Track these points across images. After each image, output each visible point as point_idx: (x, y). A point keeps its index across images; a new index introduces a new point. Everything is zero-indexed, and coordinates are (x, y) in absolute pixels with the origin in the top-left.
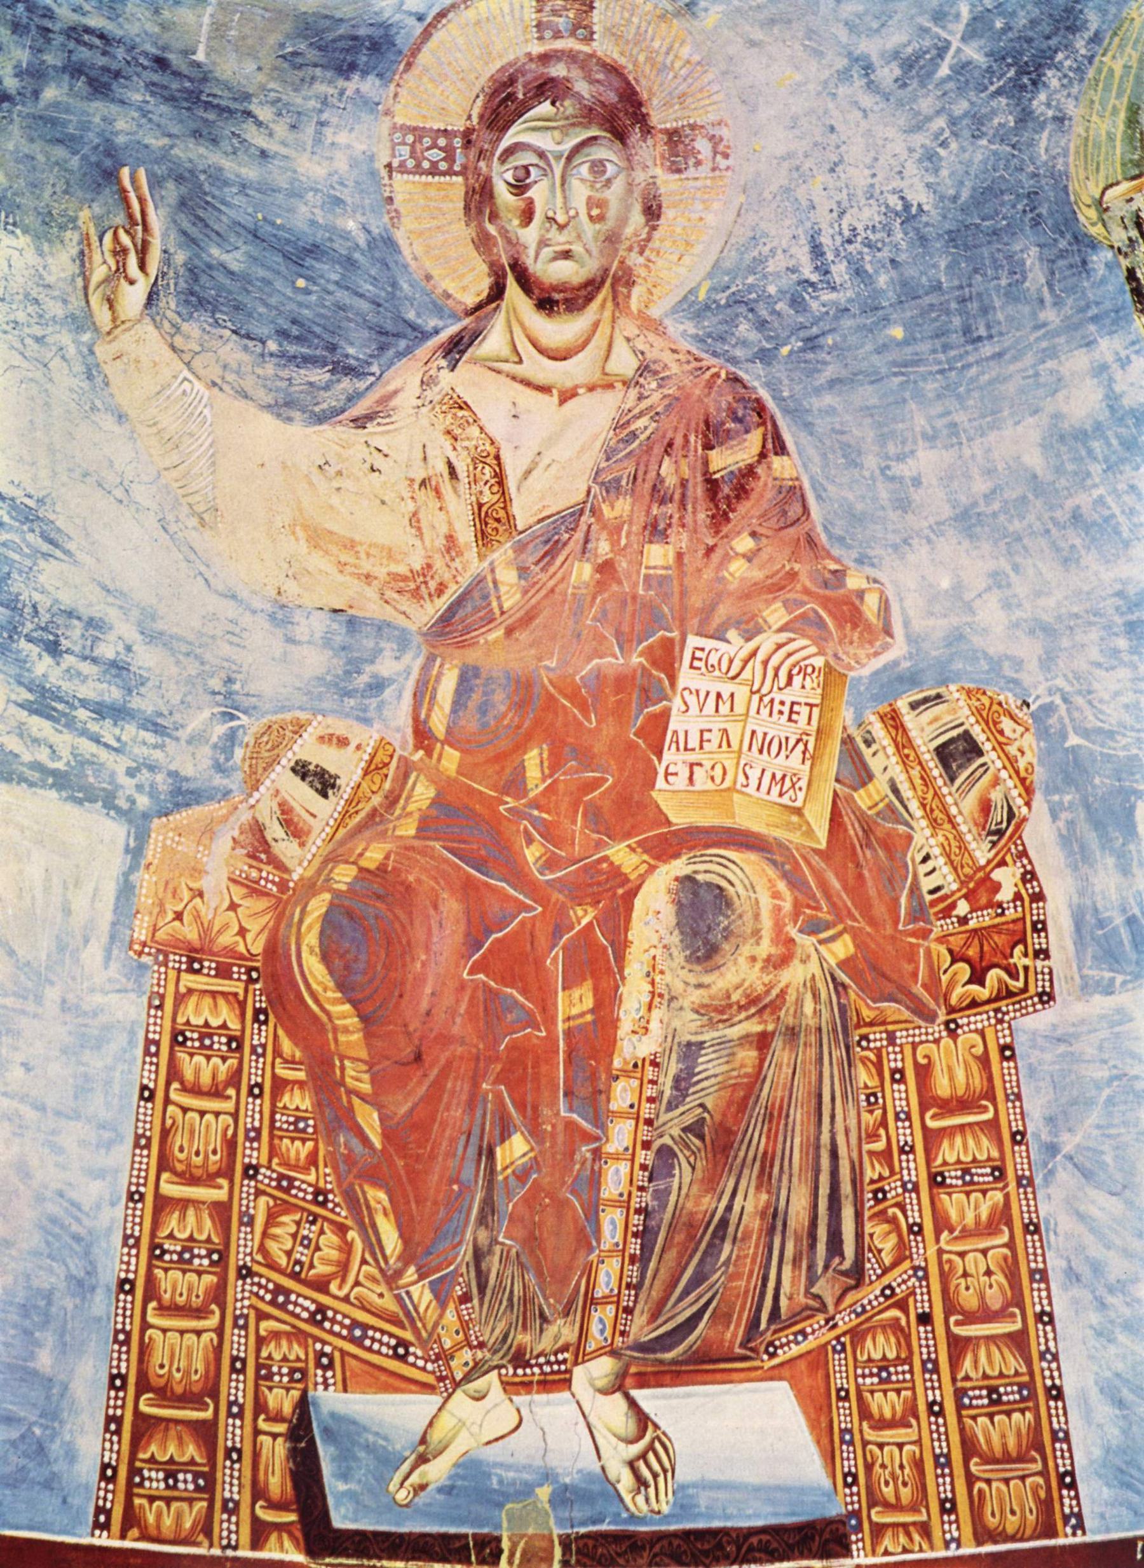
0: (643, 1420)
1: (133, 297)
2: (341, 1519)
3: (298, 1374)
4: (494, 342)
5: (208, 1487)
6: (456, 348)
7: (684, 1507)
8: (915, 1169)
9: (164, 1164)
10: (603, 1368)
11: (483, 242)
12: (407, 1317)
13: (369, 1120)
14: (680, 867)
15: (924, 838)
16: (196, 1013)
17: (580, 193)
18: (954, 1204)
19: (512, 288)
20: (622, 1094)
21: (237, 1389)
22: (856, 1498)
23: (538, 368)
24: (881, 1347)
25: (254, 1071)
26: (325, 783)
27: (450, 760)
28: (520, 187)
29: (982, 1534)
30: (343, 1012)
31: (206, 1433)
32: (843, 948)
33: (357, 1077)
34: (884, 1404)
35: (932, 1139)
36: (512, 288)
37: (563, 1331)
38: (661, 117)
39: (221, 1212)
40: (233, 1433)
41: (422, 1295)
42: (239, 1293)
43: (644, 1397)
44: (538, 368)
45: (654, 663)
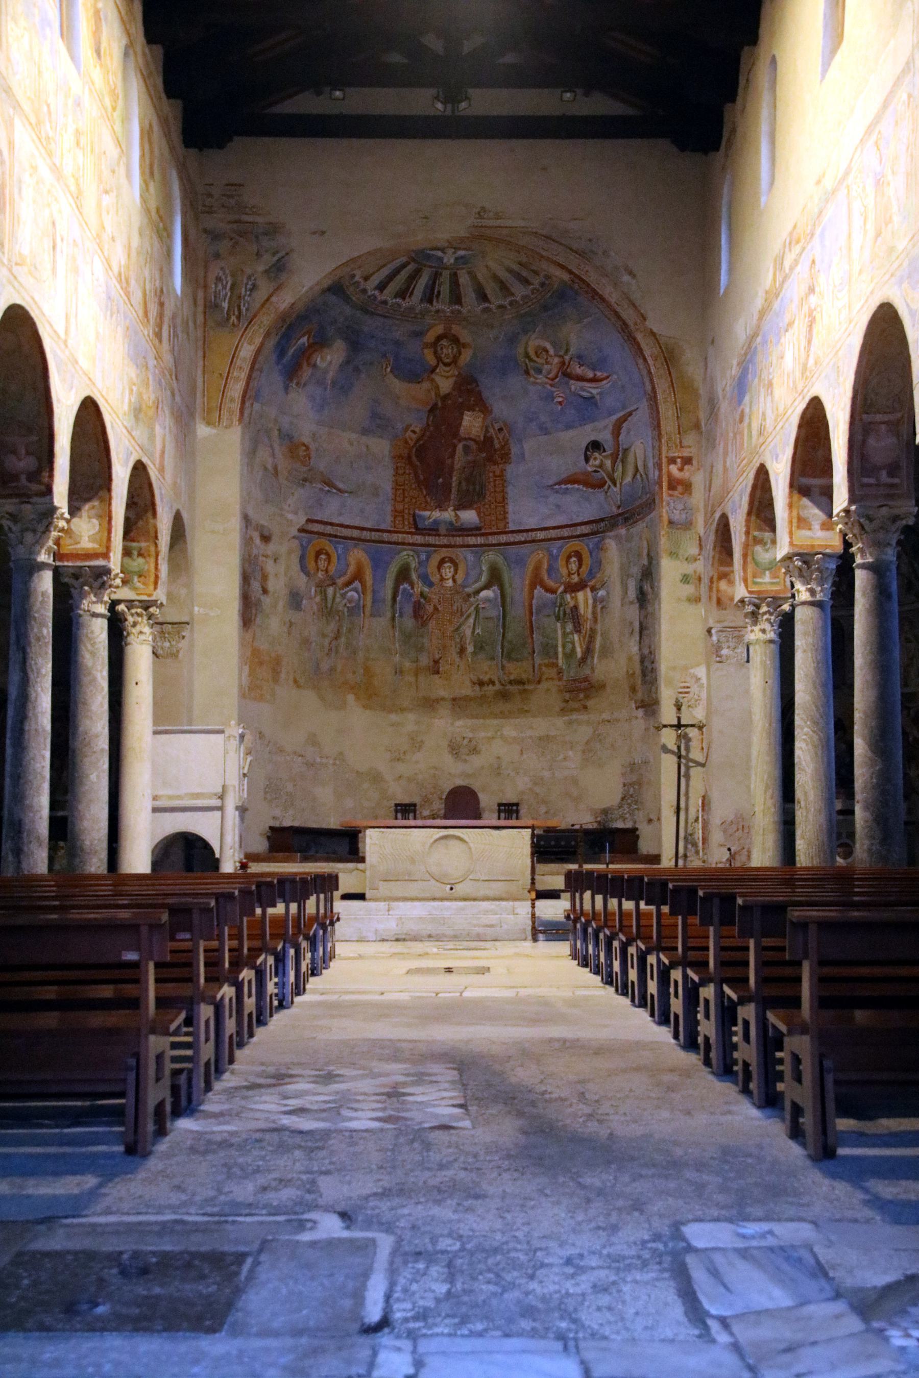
0: (456, 515)
1: (389, 370)
2: (420, 526)
3: (414, 509)
4: (438, 370)
5: (404, 523)
6: (433, 371)
7: (462, 524)
8: (492, 484)
9: (397, 484)
10: (452, 508)
11: (436, 357)
12: (427, 502)
13: (422, 477)
14: (464, 443)
15: (496, 441)
16: (399, 465)
17: (450, 351)
18: (497, 490)
19: (441, 365)
20: (455, 473)
21: (406, 511)
22: (482, 524)
23: (443, 374)
24: (487, 506)
25: (407, 471)
26: (414, 432)
27: (432, 428)
28: (442, 349)
29: (498, 529)
30: (418, 463)
31: (403, 516)
32: (484, 455)
33: (420, 472)
34: (487, 513)
35: (495, 481)
36: (441, 365)
37: (446, 504)
38: (462, 340)
39: (404, 490)
40: (406, 516)
41: (429, 500)
42: (406, 500)
43: (458, 513)
44: (443, 374)
45: (448, 498)
